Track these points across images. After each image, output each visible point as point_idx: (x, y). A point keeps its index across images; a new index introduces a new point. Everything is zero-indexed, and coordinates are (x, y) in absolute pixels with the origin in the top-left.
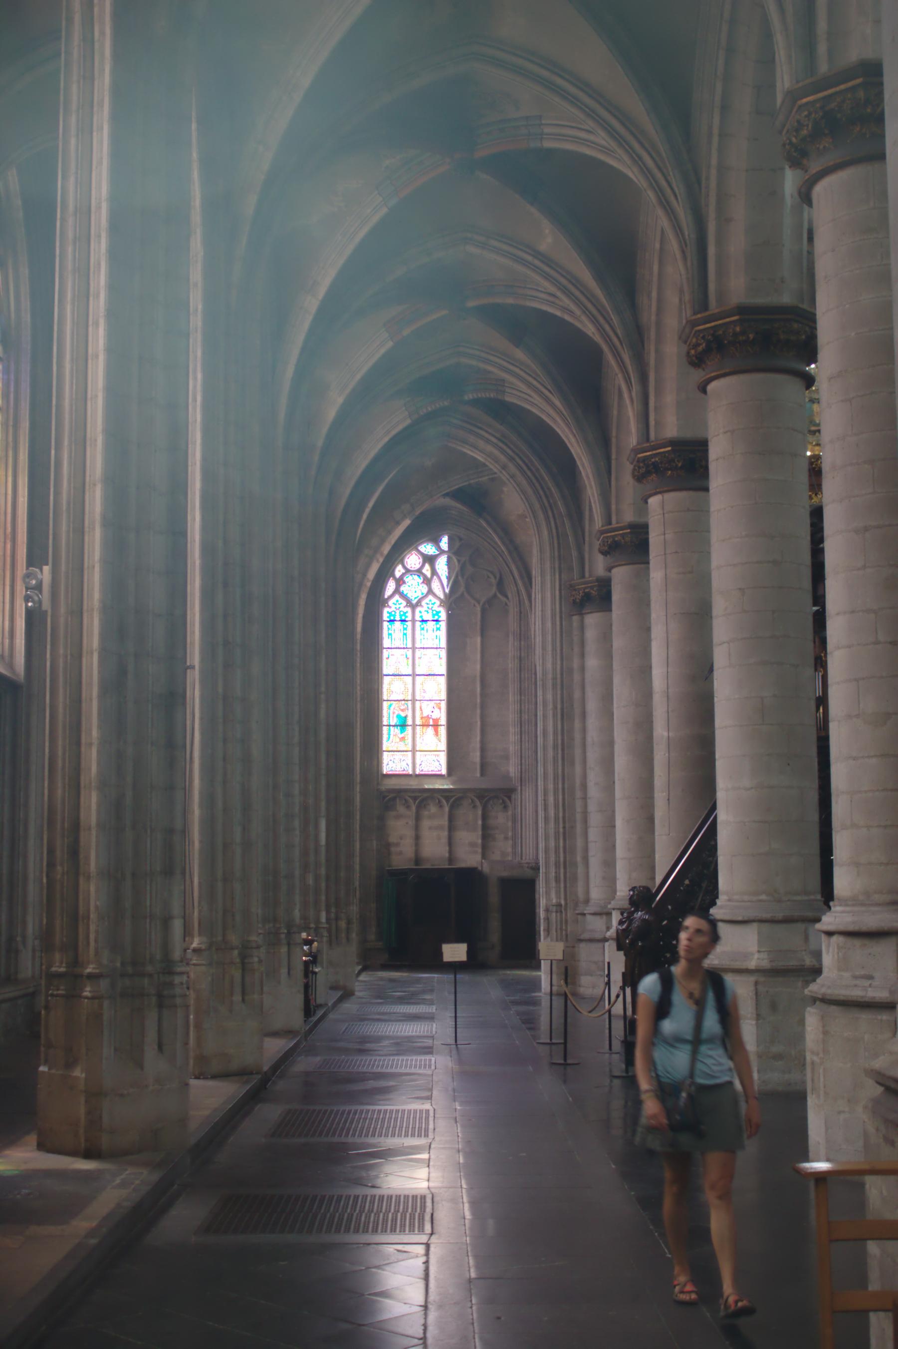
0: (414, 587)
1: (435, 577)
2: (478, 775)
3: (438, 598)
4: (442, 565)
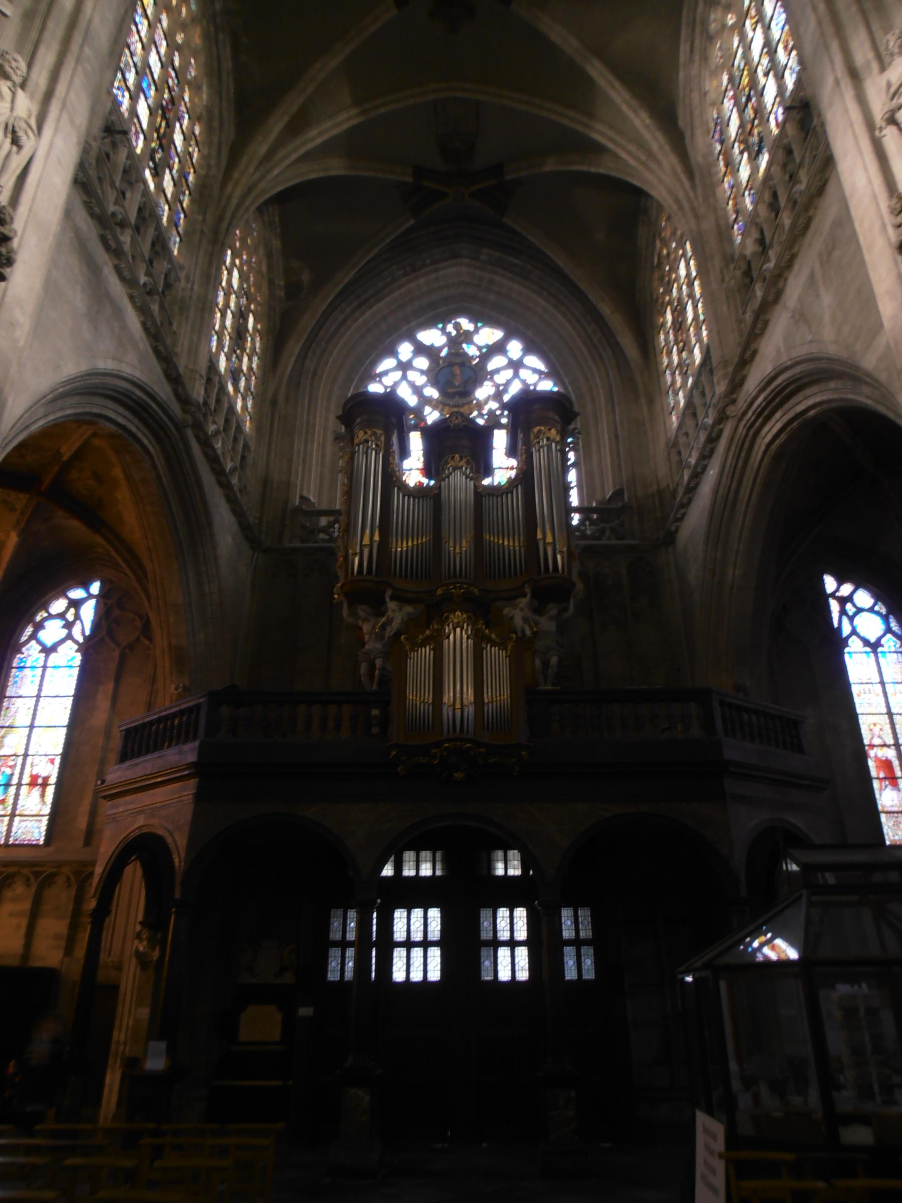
0: (52, 631)
1: (78, 622)
2: (81, 844)
3: (76, 642)
4: (88, 611)
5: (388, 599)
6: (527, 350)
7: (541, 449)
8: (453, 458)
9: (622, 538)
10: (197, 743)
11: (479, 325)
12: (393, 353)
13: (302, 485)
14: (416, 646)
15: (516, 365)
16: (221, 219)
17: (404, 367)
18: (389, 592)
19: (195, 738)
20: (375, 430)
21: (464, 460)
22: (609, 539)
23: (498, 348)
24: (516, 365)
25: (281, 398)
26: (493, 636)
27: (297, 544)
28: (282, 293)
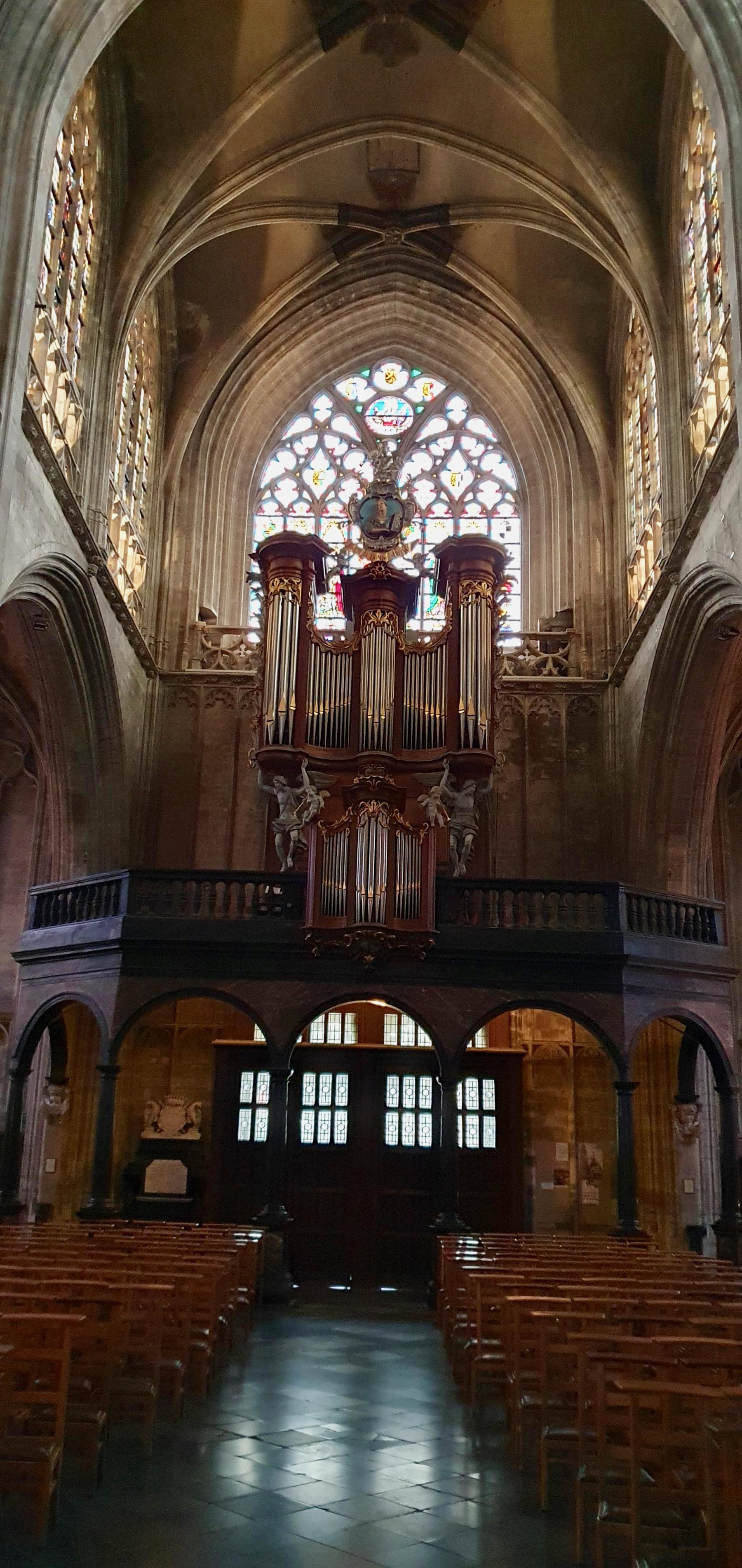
5: (304, 770)
6: (473, 410)
7: (470, 607)
8: (374, 613)
9: (564, 672)
10: (120, 919)
11: (416, 373)
12: (307, 409)
13: (202, 594)
14: (333, 832)
15: (457, 430)
16: (116, 315)
17: (321, 429)
18: (305, 763)
19: (116, 913)
20: (292, 579)
21: (387, 615)
22: (550, 674)
23: (437, 407)
24: (457, 430)
25: (175, 484)
26: (407, 824)
27: (197, 669)
28: (174, 345)
